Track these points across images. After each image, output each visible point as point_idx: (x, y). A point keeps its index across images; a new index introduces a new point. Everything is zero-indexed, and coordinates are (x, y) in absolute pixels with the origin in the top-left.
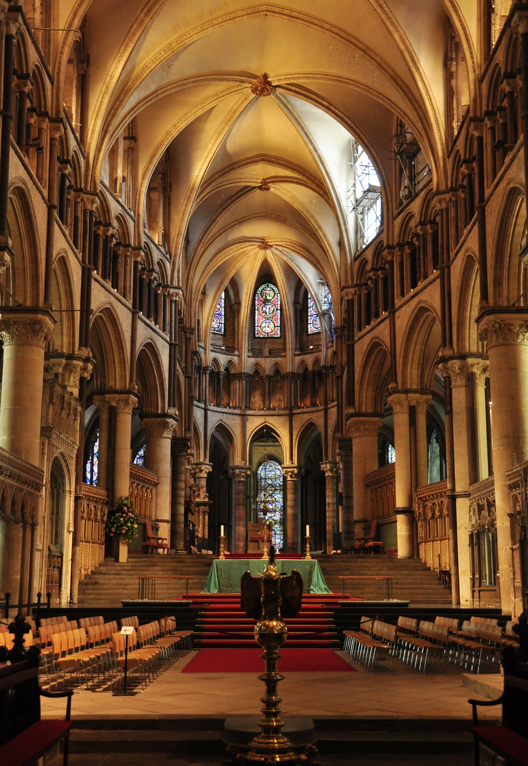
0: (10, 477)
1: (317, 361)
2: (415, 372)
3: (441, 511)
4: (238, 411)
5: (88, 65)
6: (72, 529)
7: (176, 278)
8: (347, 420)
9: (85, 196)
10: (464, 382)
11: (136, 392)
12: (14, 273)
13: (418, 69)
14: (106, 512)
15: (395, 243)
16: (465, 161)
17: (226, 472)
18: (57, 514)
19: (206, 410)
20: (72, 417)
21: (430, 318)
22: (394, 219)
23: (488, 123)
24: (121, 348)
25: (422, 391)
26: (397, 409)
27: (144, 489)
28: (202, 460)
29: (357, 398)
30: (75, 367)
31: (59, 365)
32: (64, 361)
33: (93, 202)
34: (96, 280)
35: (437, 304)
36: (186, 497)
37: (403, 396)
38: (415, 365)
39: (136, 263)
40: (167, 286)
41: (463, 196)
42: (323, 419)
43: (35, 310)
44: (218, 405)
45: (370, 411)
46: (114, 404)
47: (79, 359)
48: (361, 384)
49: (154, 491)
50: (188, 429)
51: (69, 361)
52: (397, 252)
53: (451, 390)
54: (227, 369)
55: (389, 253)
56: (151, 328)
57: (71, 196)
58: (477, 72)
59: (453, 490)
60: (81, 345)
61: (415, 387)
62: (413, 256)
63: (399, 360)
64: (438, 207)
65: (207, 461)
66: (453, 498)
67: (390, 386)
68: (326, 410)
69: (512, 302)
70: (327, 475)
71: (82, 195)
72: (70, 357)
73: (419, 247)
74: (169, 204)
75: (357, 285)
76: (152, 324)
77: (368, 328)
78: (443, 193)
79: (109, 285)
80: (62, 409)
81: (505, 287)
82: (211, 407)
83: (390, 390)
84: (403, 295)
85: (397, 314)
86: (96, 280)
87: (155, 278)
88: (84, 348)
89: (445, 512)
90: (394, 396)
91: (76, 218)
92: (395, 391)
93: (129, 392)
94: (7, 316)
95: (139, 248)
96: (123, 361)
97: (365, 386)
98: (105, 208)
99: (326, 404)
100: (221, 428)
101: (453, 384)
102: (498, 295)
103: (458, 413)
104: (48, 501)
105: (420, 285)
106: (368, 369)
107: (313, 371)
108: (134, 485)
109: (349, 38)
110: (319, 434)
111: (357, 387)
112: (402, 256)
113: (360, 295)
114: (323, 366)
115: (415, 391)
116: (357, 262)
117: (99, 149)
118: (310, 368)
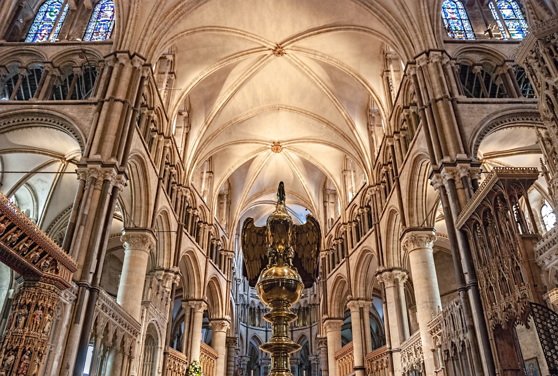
0: (113, 317)
1: (306, 301)
2: (362, 289)
3: (382, 365)
4: (265, 329)
5: (190, 129)
6: (160, 371)
7: (231, 247)
8: (324, 322)
9: (183, 189)
10: (392, 285)
11: (206, 300)
12: (135, 209)
13: (354, 128)
14: (185, 368)
15: (347, 222)
16: (384, 165)
17: (257, 364)
18: (153, 362)
19: (247, 327)
20: (164, 301)
21: (369, 256)
22: (346, 210)
23: (396, 137)
24: (199, 276)
25: (366, 300)
26: (352, 309)
27: (209, 359)
28: (244, 354)
29: (329, 310)
30: (170, 276)
31: (161, 275)
32: (163, 273)
33: (187, 192)
34: (186, 233)
35: (373, 246)
36: (234, 371)
37: (356, 302)
38: (361, 285)
39: (209, 232)
40: (227, 251)
41: (383, 187)
42: (309, 333)
43: (144, 230)
44: (254, 325)
45: (336, 316)
46: (193, 307)
47: (173, 272)
48: (331, 302)
49: (215, 362)
50: (236, 333)
51: (167, 273)
52: (348, 226)
53: (385, 289)
54: (259, 307)
55: (344, 227)
56: (217, 269)
57: (175, 187)
58: (387, 116)
59: (391, 348)
60: (174, 265)
61: (362, 297)
62: (357, 227)
63: (353, 282)
64: (371, 194)
65: (247, 355)
66: (391, 353)
67: (348, 297)
68: (311, 327)
69: (420, 225)
70: (312, 362)
71: (181, 187)
72: (167, 271)
73: (360, 221)
74: (229, 210)
75: (327, 250)
76: (218, 267)
77: (334, 270)
78: (372, 186)
79: (194, 239)
80: (158, 293)
81: (415, 216)
82: (250, 326)
83: (348, 299)
84: (353, 247)
85: (350, 258)
86: (186, 233)
87: (220, 245)
88: (175, 267)
89: (385, 365)
90: (351, 302)
91: (177, 199)
92: (351, 299)
93: (202, 300)
94: (129, 233)
95: (212, 225)
96: (199, 283)
97: (333, 303)
98: (195, 201)
99: (311, 324)
100: (255, 337)
101: (386, 286)
102: (411, 222)
103: (390, 303)
104: (143, 347)
105: (362, 239)
106: (335, 293)
107: (304, 308)
108: (203, 356)
109: (320, 118)
110: (308, 342)
111: (329, 304)
112: (351, 228)
113: (329, 255)
114: (309, 304)
115: (362, 299)
116: (327, 238)
117: (192, 167)
118: (302, 306)
